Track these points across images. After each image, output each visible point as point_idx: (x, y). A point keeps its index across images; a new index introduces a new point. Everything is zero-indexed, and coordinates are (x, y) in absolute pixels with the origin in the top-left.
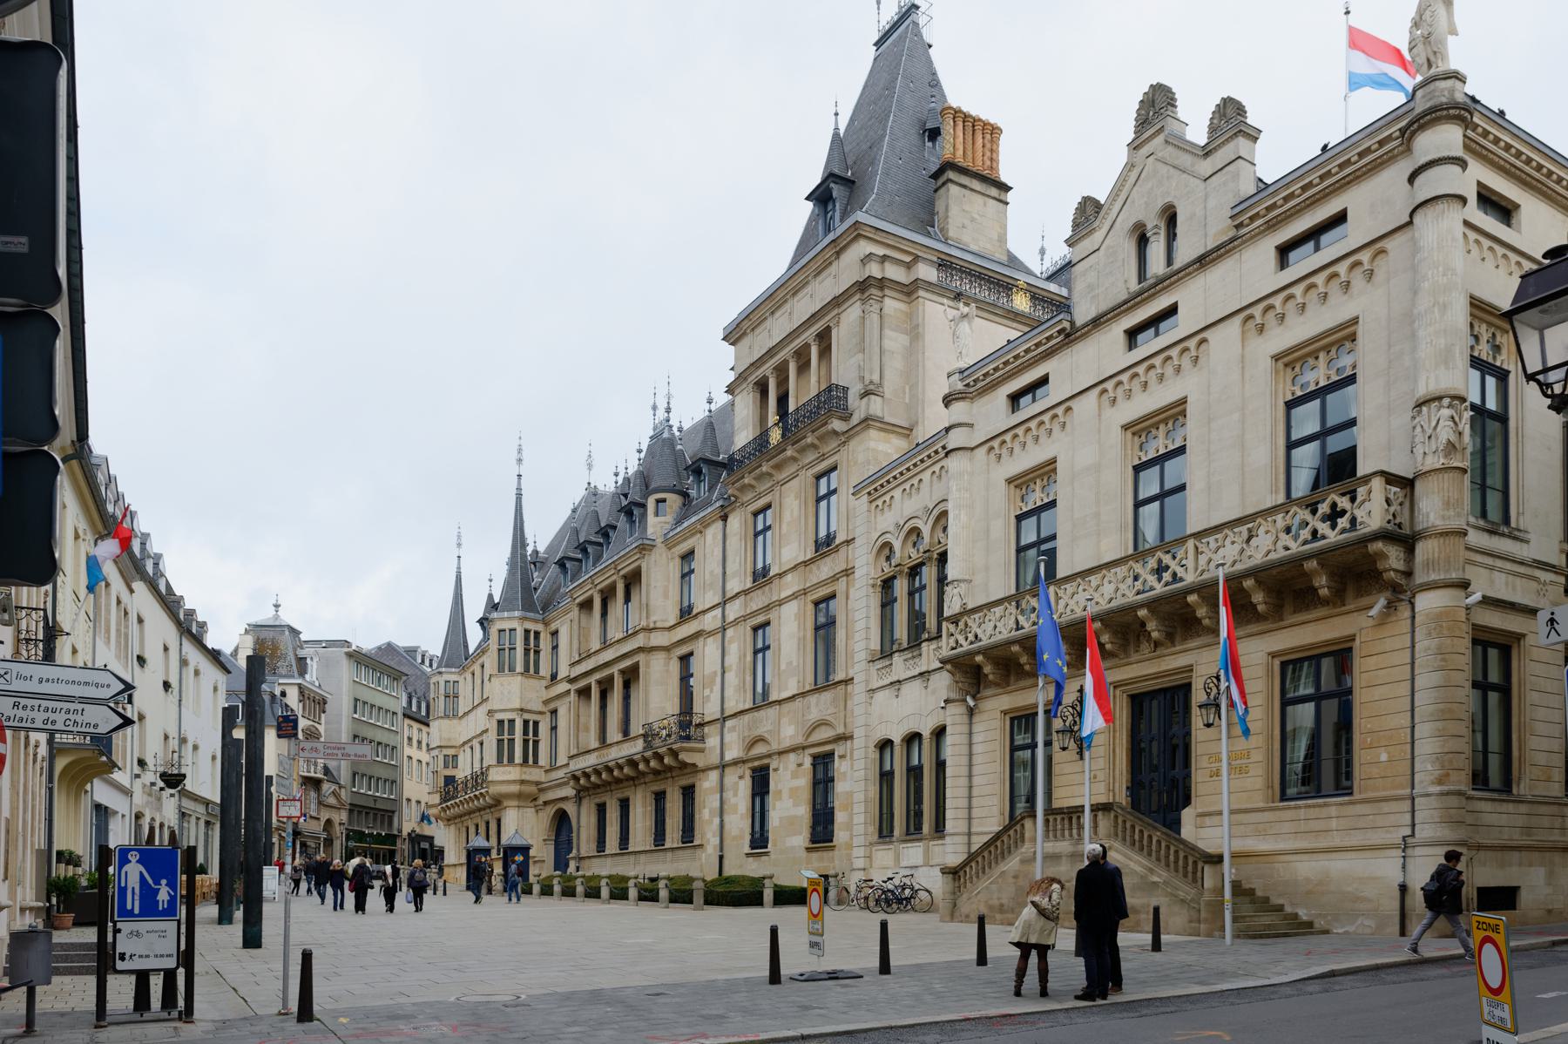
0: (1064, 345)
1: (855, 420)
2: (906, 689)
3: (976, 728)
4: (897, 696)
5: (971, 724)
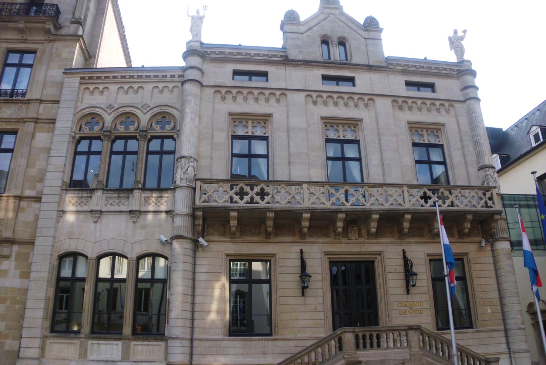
0: (281, 63)
1: (63, 32)
2: (106, 220)
3: (198, 262)
4: (96, 222)
5: (195, 258)
